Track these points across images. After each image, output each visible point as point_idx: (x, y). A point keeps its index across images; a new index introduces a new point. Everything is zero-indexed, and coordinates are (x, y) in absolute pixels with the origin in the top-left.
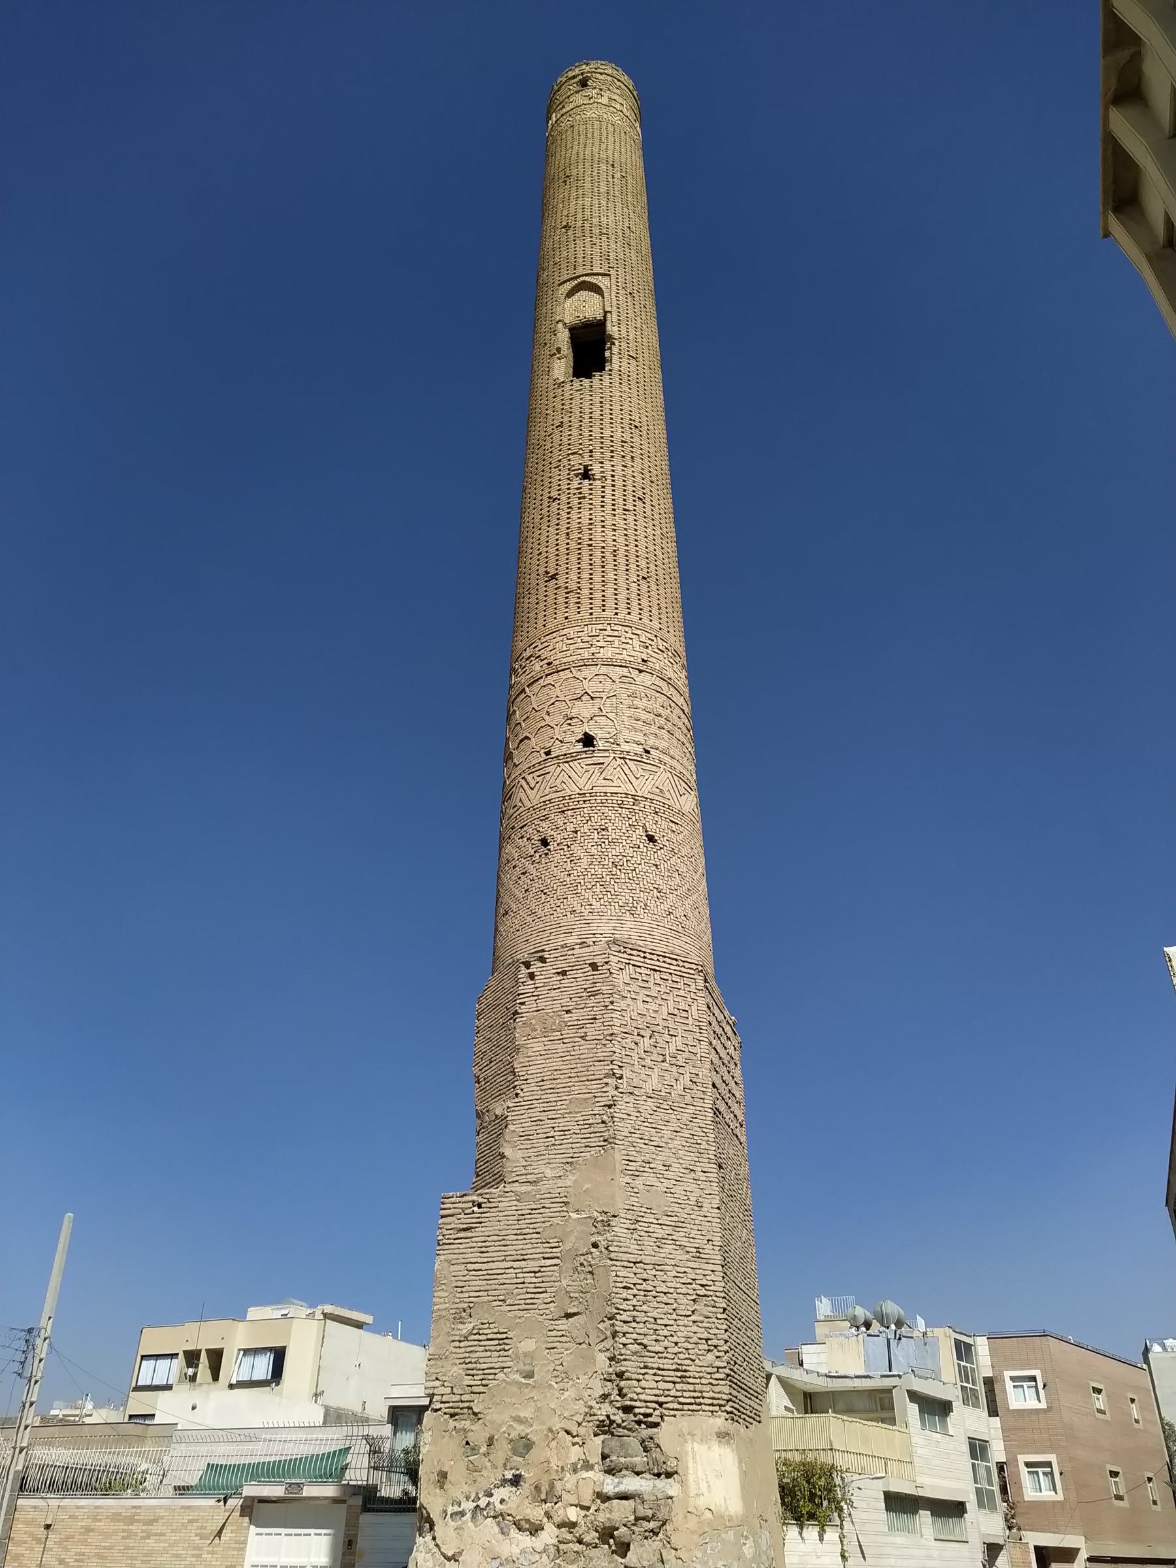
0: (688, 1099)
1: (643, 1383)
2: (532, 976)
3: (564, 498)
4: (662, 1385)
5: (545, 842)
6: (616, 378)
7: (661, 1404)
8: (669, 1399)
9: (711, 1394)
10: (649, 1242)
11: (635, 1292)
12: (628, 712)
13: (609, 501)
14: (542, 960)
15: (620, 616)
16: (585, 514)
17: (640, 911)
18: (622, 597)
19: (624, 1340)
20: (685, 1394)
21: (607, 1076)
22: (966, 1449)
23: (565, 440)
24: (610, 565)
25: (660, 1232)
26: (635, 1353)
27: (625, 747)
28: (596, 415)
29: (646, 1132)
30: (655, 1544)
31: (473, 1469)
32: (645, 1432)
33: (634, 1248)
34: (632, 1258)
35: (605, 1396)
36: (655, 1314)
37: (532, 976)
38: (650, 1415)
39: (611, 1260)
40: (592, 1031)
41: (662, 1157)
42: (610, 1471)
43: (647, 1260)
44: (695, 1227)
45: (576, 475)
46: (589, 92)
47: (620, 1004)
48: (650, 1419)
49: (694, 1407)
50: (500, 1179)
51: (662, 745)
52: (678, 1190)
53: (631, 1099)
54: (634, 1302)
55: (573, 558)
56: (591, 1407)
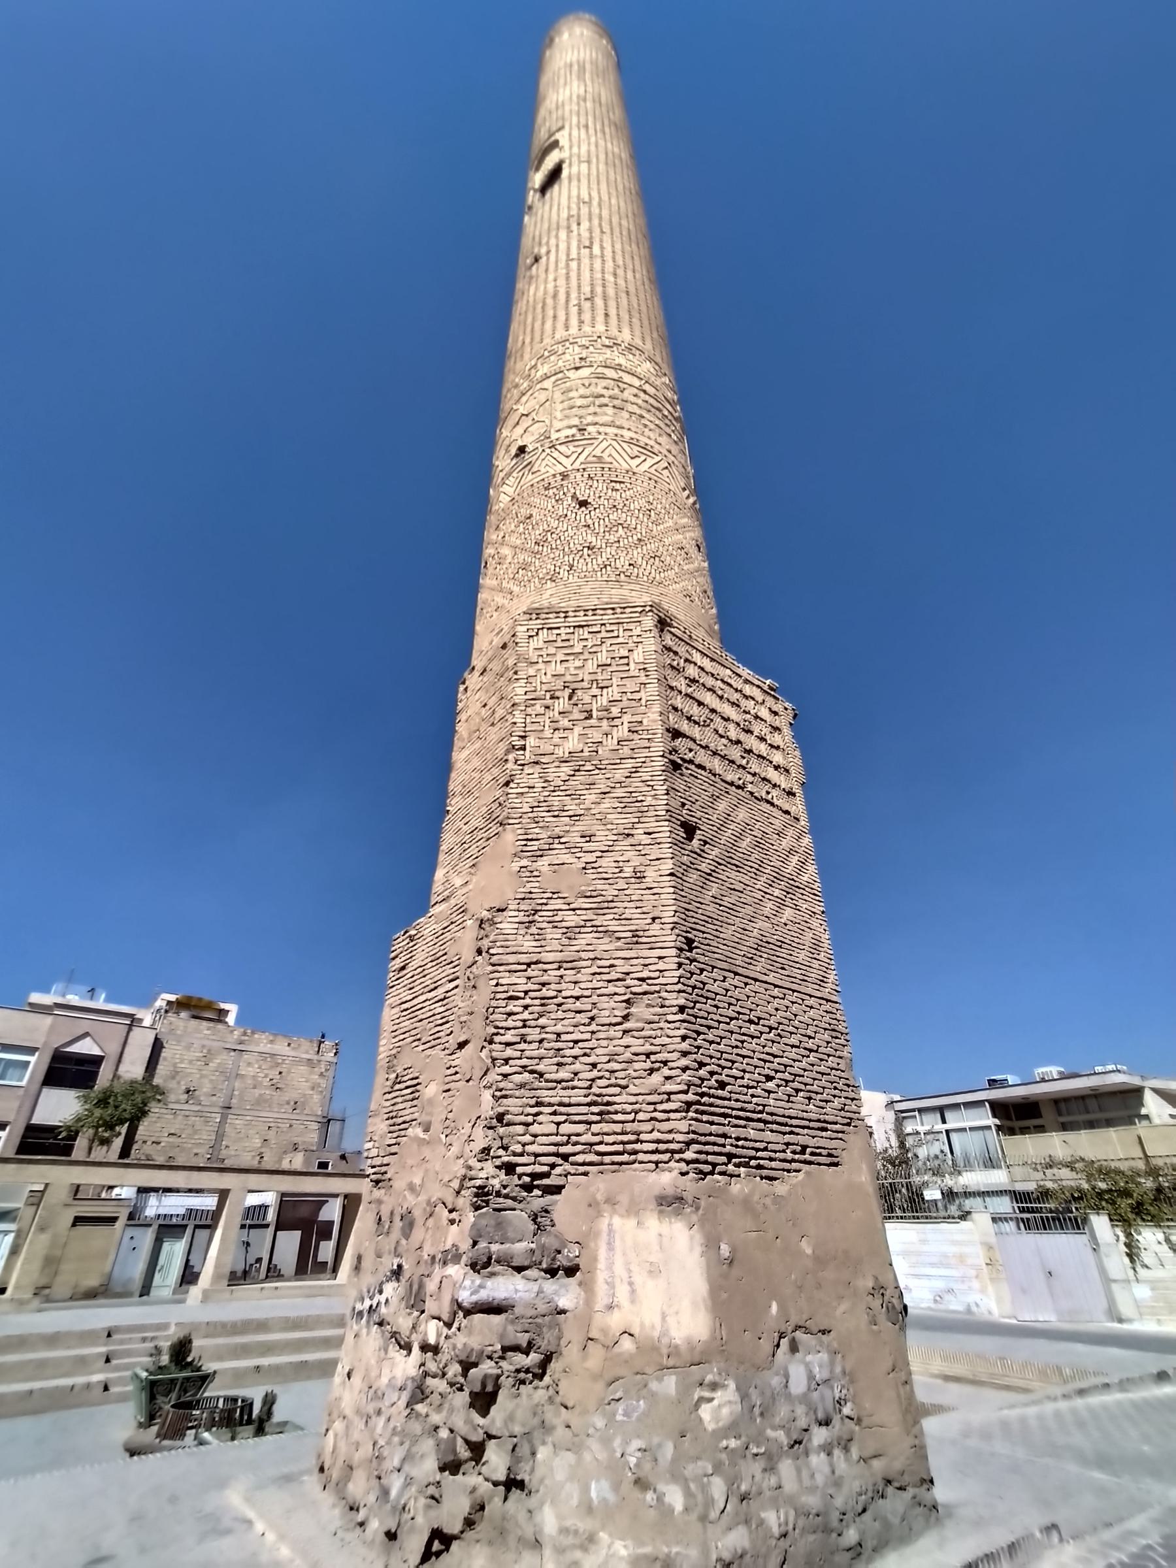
0: (626, 751)
1: (535, 1129)
4: (566, 1128)
7: (565, 1157)
8: (579, 1148)
9: (656, 1135)
10: (551, 934)
11: (528, 1001)
17: (564, 574)
19: (506, 1069)
20: (607, 1139)
21: (507, 752)
25: (572, 919)
26: (522, 1086)
29: (555, 802)
30: (534, 1394)
32: (537, 1201)
33: (528, 944)
34: (524, 958)
35: (486, 1150)
36: (559, 1028)
38: (547, 1175)
39: (494, 965)
43: (550, 957)
44: (632, 905)
47: (526, 671)
48: (546, 1182)
49: (625, 1158)
53: (538, 769)
54: (526, 1015)
56: (470, 1168)
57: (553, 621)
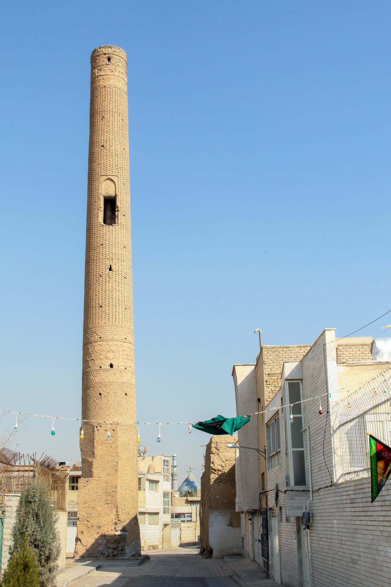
3: (104, 276)
6: (120, 226)
12: (122, 356)
13: (117, 280)
14: (101, 426)
16: (111, 285)
18: (120, 317)
22: (162, 495)
23: (104, 252)
24: (117, 306)
25: (125, 488)
27: (121, 368)
31: (88, 531)
37: (98, 430)
40: (113, 445)
42: (116, 531)
46: (111, 67)
50: (91, 476)
51: (129, 365)
52: (129, 479)
55: (107, 301)
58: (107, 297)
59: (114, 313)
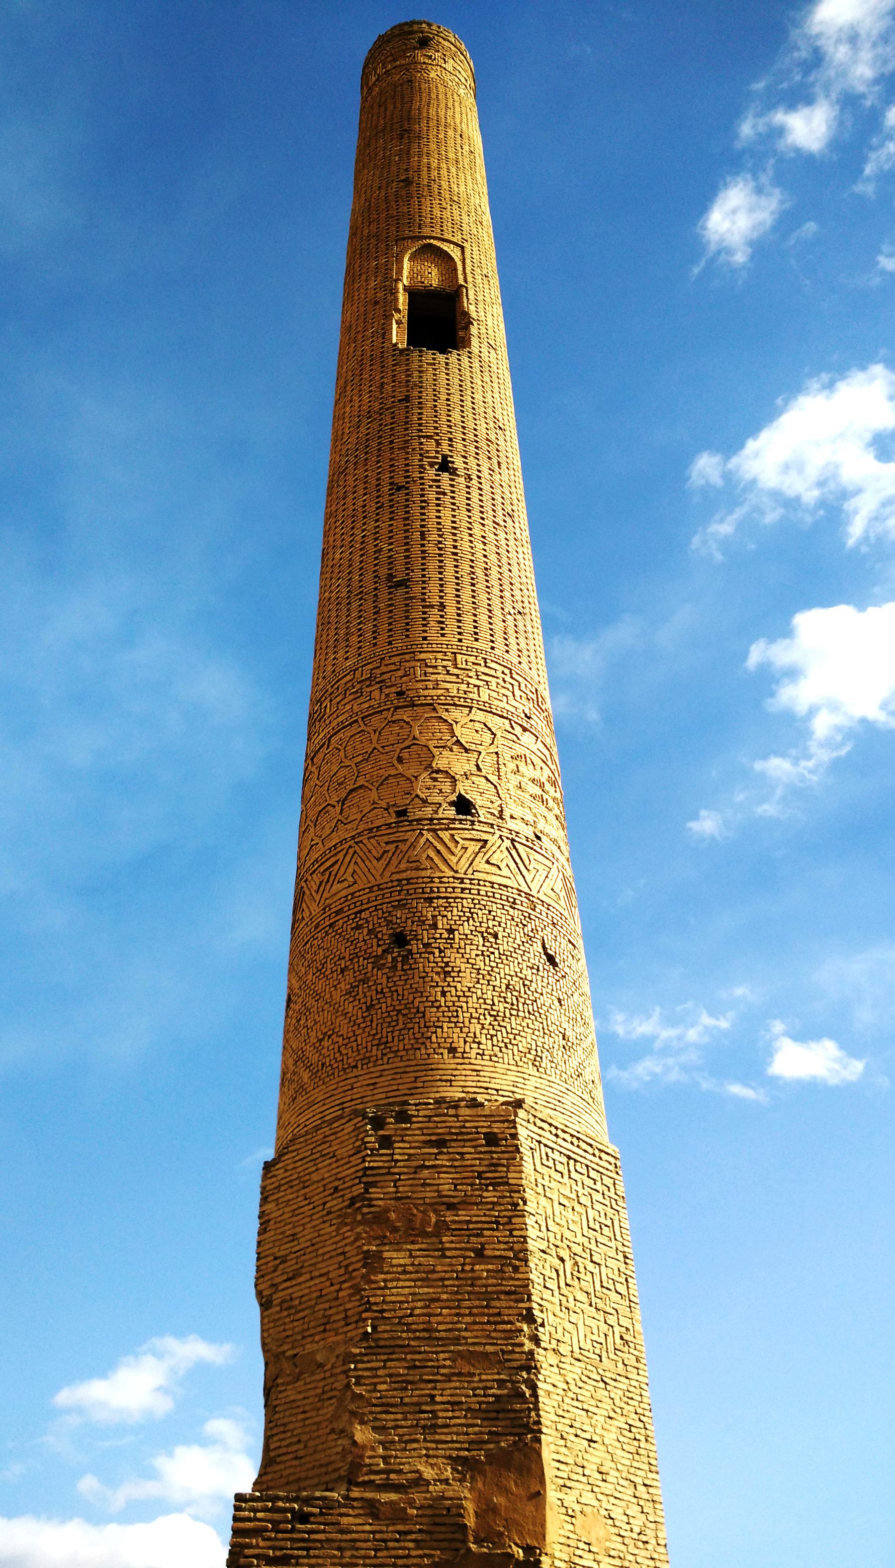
2: (386, 1142)
5: (400, 940)
12: (514, 780)
15: (497, 652)
16: (446, 514)
24: (481, 586)
28: (455, 398)
41: (596, 1456)
45: (432, 465)
52: (617, 1513)
55: (432, 565)
57: (548, 1138)
58: (432, 550)
59: (468, 607)
